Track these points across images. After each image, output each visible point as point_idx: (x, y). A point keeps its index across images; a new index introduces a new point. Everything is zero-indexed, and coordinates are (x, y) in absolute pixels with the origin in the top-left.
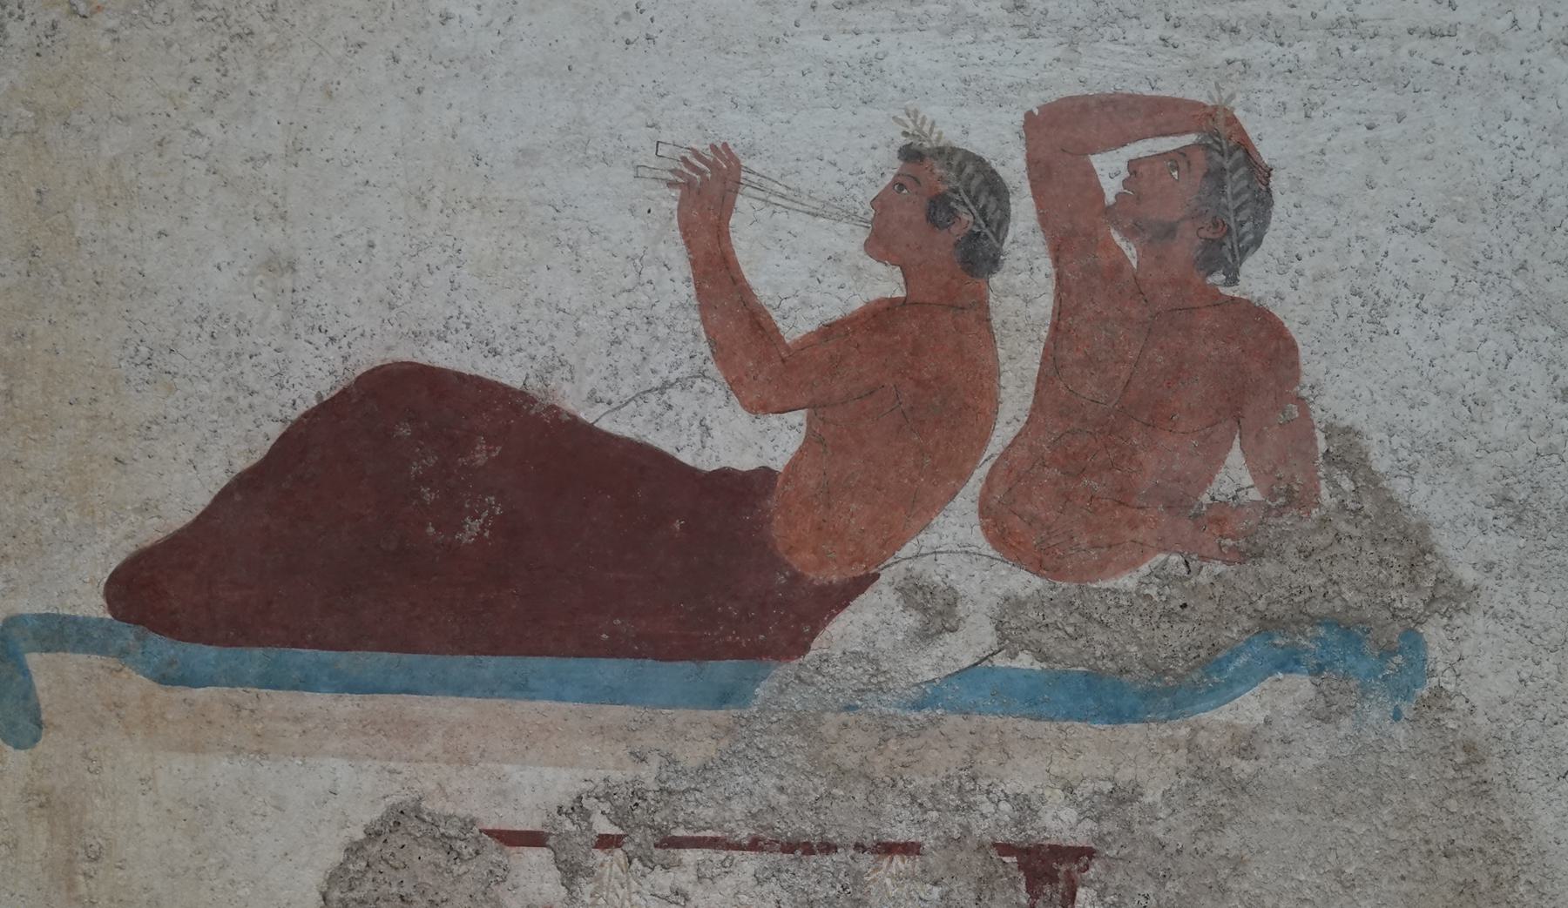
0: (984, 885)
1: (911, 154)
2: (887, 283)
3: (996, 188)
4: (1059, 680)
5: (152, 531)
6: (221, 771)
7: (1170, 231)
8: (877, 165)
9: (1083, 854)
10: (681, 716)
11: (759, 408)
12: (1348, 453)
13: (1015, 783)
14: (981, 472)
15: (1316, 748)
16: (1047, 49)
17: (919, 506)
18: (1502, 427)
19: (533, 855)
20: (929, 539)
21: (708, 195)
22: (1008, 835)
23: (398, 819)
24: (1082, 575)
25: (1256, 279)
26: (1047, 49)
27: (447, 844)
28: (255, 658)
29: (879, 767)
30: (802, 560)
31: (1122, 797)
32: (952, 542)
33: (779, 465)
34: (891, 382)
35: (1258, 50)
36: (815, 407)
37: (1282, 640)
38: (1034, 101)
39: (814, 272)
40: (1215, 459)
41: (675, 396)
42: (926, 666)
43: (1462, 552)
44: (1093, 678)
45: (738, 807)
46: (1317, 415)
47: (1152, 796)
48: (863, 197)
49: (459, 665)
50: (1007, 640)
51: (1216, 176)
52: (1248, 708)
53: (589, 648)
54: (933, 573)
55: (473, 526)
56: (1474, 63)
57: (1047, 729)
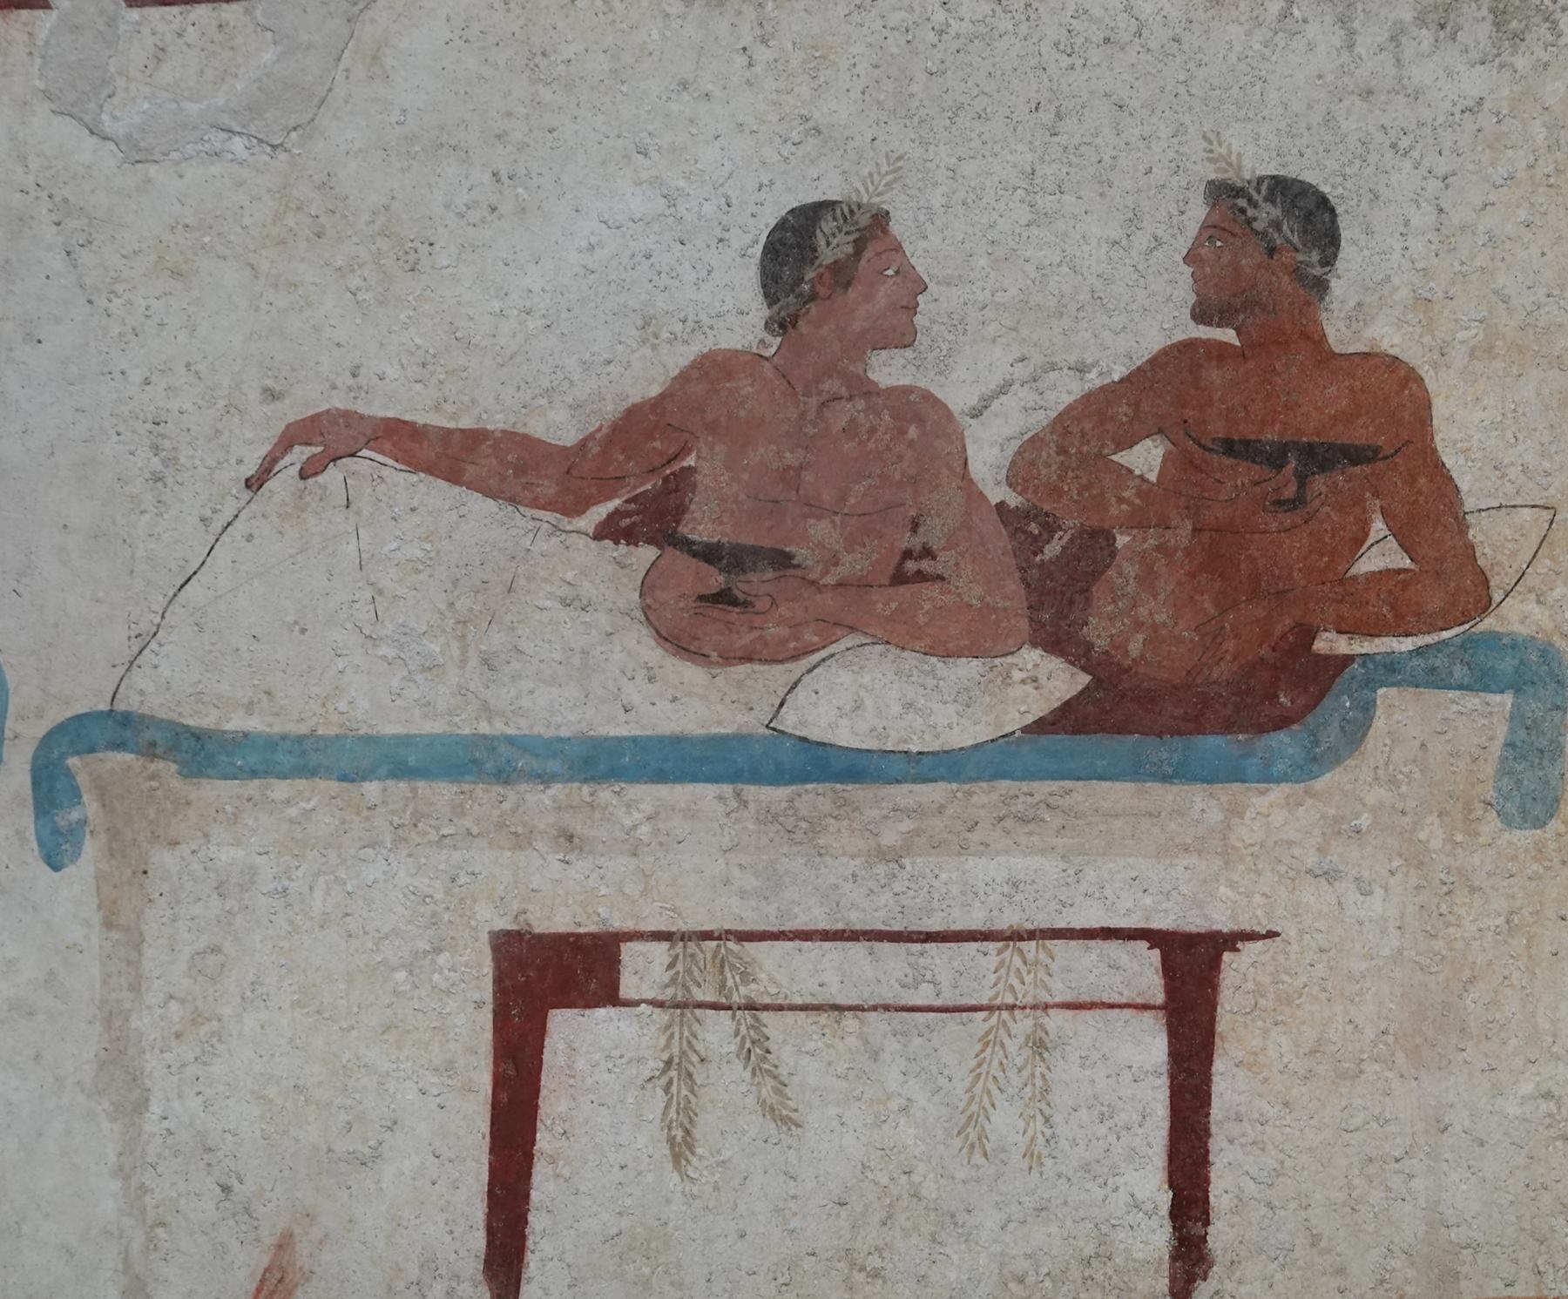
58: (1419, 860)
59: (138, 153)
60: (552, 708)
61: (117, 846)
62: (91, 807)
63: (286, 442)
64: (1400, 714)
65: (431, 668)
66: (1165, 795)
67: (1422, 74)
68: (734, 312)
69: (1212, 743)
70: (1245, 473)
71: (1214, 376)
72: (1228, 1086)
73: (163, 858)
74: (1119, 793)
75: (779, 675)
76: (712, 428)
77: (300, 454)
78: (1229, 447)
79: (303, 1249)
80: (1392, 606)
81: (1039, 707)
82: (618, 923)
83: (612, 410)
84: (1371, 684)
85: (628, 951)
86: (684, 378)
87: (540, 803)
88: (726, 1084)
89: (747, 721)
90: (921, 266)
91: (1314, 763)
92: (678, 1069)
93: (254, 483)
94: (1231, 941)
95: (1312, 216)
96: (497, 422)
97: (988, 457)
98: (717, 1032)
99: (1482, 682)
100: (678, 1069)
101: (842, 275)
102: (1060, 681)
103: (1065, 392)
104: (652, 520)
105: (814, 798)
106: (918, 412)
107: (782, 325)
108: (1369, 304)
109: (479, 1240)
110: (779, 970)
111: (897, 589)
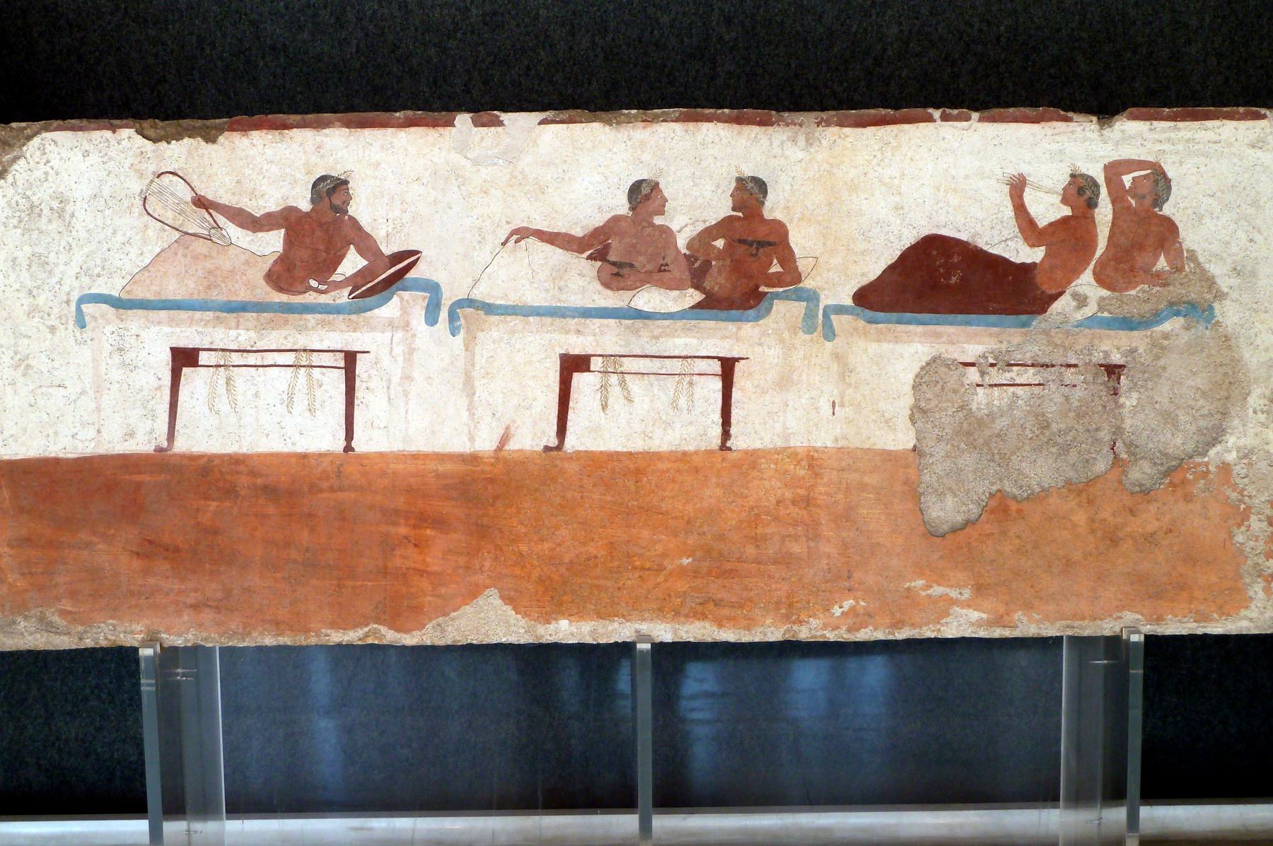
1: (1073, 176)
2: (1067, 211)
3: (1096, 185)
4: (1114, 319)
5: (865, 281)
6: (886, 347)
7: (1144, 197)
10: (1012, 330)
11: (1032, 246)
12: (1193, 256)
13: (1104, 348)
14: (1093, 263)
15: (1185, 337)
16: (1110, 146)
17: (1076, 272)
18: (1234, 249)
19: (973, 369)
20: (1079, 281)
21: (1017, 187)
22: (1102, 362)
24: (1121, 291)
25: (1167, 210)
26: (1110, 146)
27: (948, 366)
28: (895, 316)
29: (1067, 343)
30: (1044, 287)
31: (1133, 351)
32: (1085, 281)
33: (1038, 261)
34: (1069, 237)
35: (1167, 147)
37: (1175, 308)
38: (1107, 161)
39: (1047, 208)
40: (1157, 258)
41: (1009, 243)
42: (1079, 316)
43: (1223, 284)
44: (1125, 319)
45: (1028, 355)
46: (1184, 247)
48: (1060, 188)
49: (951, 317)
50: (1101, 309)
51: (1156, 182)
52: (1167, 326)
53: (986, 312)
54: (1080, 290)
55: (954, 280)
56: (1226, 150)
58: (782, 341)
59: (476, 162)
60: (576, 301)
61: (468, 331)
62: (462, 321)
63: (512, 234)
64: (779, 307)
65: (547, 290)
67: (788, 153)
68: (621, 206)
69: (733, 312)
70: (744, 247)
71: (737, 224)
72: (736, 394)
73: (480, 335)
74: (711, 324)
75: (630, 293)
76: (616, 234)
77: (515, 237)
78: (742, 241)
79: (512, 430)
80: (778, 280)
82: (590, 352)
83: (591, 228)
84: (773, 299)
85: (593, 360)
86: (609, 221)
87: (572, 323)
88: (615, 391)
89: (620, 304)
90: (666, 195)
91: (758, 318)
92: (604, 388)
94: (738, 360)
95: (761, 186)
96: (563, 231)
97: (682, 243)
98: (614, 379)
99: (799, 299)
100: (604, 388)
101: (647, 197)
102: (697, 297)
103: (701, 227)
104: (600, 256)
106: (666, 232)
107: (633, 209)
108: (773, 208)
110: (629, 365)
111: (659, 275)
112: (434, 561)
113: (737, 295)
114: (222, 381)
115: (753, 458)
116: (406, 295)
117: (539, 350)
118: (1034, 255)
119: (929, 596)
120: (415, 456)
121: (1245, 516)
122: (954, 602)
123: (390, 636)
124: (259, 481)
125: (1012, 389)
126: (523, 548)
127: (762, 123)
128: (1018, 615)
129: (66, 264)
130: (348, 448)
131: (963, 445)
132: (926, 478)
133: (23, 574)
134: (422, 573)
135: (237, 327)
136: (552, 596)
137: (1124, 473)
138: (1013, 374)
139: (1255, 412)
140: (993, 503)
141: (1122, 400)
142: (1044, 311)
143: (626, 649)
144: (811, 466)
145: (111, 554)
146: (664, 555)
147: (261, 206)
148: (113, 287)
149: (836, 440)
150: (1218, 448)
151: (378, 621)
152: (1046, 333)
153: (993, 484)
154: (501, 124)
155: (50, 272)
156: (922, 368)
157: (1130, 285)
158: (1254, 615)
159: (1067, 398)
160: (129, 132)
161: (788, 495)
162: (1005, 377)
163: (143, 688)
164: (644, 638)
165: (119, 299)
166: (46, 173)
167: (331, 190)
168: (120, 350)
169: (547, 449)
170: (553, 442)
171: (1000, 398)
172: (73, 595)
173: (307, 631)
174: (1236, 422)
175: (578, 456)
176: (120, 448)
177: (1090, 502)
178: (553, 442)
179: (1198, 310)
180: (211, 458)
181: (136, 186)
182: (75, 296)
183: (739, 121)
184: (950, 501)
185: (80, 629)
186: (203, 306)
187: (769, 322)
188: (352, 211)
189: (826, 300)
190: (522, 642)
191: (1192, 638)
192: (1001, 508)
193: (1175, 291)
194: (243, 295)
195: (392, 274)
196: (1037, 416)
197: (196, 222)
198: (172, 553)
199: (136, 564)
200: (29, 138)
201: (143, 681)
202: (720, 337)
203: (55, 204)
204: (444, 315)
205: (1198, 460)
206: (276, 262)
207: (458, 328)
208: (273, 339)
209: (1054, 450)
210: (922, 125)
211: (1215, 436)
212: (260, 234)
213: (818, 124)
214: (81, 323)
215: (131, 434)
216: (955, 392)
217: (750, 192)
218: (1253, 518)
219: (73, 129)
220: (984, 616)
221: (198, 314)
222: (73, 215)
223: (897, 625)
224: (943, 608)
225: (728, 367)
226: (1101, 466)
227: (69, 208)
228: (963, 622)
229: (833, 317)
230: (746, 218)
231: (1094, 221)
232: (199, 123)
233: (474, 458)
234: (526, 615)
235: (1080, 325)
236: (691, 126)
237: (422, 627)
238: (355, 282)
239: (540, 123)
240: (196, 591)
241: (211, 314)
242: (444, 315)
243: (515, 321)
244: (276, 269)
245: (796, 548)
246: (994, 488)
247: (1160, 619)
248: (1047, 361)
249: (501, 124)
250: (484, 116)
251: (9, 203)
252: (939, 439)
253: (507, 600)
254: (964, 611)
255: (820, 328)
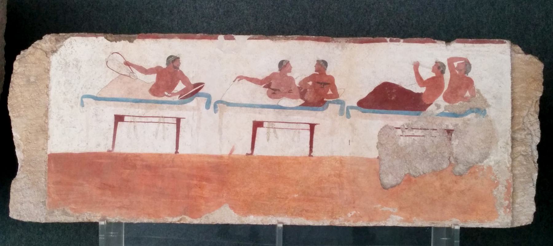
0: (443, 133)
1: (436, 62)
3: (444, 66)
8: (433, 63)
9: (453, 130)
11: (421, 87)
12: (479, 91)
15: (475, 120)
17: (436, 96)
21: (416, 66)
23: (386, 126)
24: (453, 103)
25: (470, 75)
28: (372, 110)
30: (425, 102)
31: (456, 125)
32: (440, 100)
34: (434, 84)
36: (427, 87)
37: (472, 110)
38: (448, 57)
39: (427, 74)
40: (466, 92)
42: (438, 112)
43: (490, 101)
47: (460, 125)
49: (392, 111)
50: (445, 110)
51: (466, 65)
52: (469, 116)
53: (405, 110)
54: (439, 103)
55: (393, 98)
57: (449, 118)
60: (259, 102)
64: (331, 106)
66: (310, 111)
68: (276, 69)
69: (315, 108)
70: (319, 85)
71: (317, 76)
78: (318, 83)
80: (331, 97)
81: (300, 104)
82: (264, 120)
83: (265, 77)
85: (264, 123)
87: (257, 110)
88: (272, 135)
91: (323, 110)
93: (234, 81)
95: (325, 63)
96: (255, 77)
97: (297, 82)
98: (272, 130)
99: (338, 104)
100: (268, 133)
101: (285, 66)
103: (304, 77)
104: (268, 86)
105: (281, 111)
106: (291, 79)
107: (280, 70)
108: (330, 71)
109: (250, 147)
110: (277, 125)
111: (289, 93)
112: (206, 193)
113: (316, 101)
114: (132, 127)
115: (320, 160)
116: (199, 98)
117: (246, 119)
118: (421, 90)
119: (383, 211)
120: (200, 156)
121: (497, 185)
122: (391, 213)
123: (188, 220)
124: (144, 163)
125: (413, 137)
126: (238, 189)
127: (326, 41)
128: (414, 218)
129: (78, 84)
130: (177, 152)
131: (395, 157)
132: (383, 168)
133: (58, 195)
134: (201, 197)
135: (139, 108)
136: (248, 207)
137: (454, 168)
138: (414, 132)
139: (501, 148)
140: (406, 178)
141: (453, 142)
142: (425, 110)
143: (273, 227)
144: (341, 163)
145: (89, 188)
146: (288, 193)
147: (147, 66)
148: (95, 93)
149: (350, 154)
150: (487, 160)
151: (185, 214)
152: (426, 117)
153: (406, 171)
154: (234, 39)
155: (72, 87)
156: (381, 129)
157: (456, 101)
158: (500, 221)
159: (433, 141)
160: (103, 38)
161: (333, 173)
162: (411, 133)
163: (100, 238)
164: (280, 223)
165: (97, 97)
166: (72, 51)
167: (173, 61)
168: (96, 115)
169: (247, 154)
170: (250, 152)
171: (409, 140)
172: (75, 203)
173: (159, 217)
174: (494, 151)
175: (259, 157)
176: (94, 150)
177: (441, 178)
178: (250, 152)
179: (480, 111)
180: (127, 154)
181: (104, 57)
182: (81, 95)
183: (318, 40)
184: (390, 177)
185: (77, 215)
186: (127, 100)
187: (327, 111)
188: (181, 68)
189: (348, 104)
190: (237, 223)
191: (477, 229)
192: (409, 179)
193: (473, 104)
194: (141, 97)
195: (194, 91)
196: (422, 147)
197: (125, 70)
198: (111, 188)
199: (99, 192)
200: (66, 39)
201: (100, 235)
202: (309, 116)
203: (75, 63)
204: (212, 106)
205: (480, 164)
206: (153, 86)
207: (217, 111)
208: (151, 113)
209: (428, 159)
210: (383, 43)
211: (486, 156)
212: (148, 75)
213: (346, 42)
214: (82, 105)
215: (99, 145)
216: (393, 138)
217: (322, 65)
218: (500, 186)
219: (82, 36)
220: (402, 218)
221: (124, 103)
222: (81, 67)
223: (371, 220)
224: (387, 215)
225: (312, 127)
226: (445, 166)
227: (80, 64)
228: (395, 219)
229: (350, 110)
230: (320, 74)
231: (443, 79)
232: (127, 36)
233: (221, 157)
234: (238, 213)
235: (438, 115)
236: (301, 41)
237: (200, 217)
238: (181, 93)
239: (248, 39)
240: (120, 202)
241: (129, 103)
242: (212, 106)
243: (237, 109)
244: (154, 88)
245: (335, 192)
246: (407, 172)
247: (466, 221)
248: (426, 127)
249: (234, 39)
250: (229, 36)
251: (58, 62)
252: (387, 154)
253: (232, 208)
254: (395, 216)
255: (345, 114)
